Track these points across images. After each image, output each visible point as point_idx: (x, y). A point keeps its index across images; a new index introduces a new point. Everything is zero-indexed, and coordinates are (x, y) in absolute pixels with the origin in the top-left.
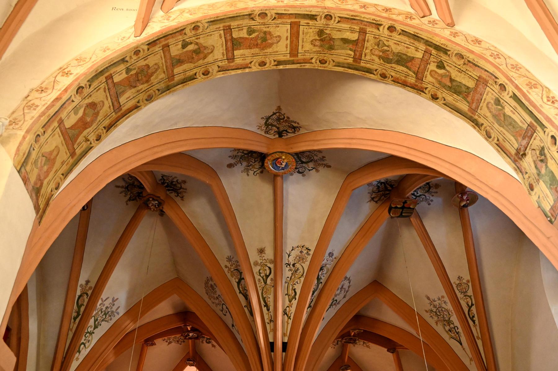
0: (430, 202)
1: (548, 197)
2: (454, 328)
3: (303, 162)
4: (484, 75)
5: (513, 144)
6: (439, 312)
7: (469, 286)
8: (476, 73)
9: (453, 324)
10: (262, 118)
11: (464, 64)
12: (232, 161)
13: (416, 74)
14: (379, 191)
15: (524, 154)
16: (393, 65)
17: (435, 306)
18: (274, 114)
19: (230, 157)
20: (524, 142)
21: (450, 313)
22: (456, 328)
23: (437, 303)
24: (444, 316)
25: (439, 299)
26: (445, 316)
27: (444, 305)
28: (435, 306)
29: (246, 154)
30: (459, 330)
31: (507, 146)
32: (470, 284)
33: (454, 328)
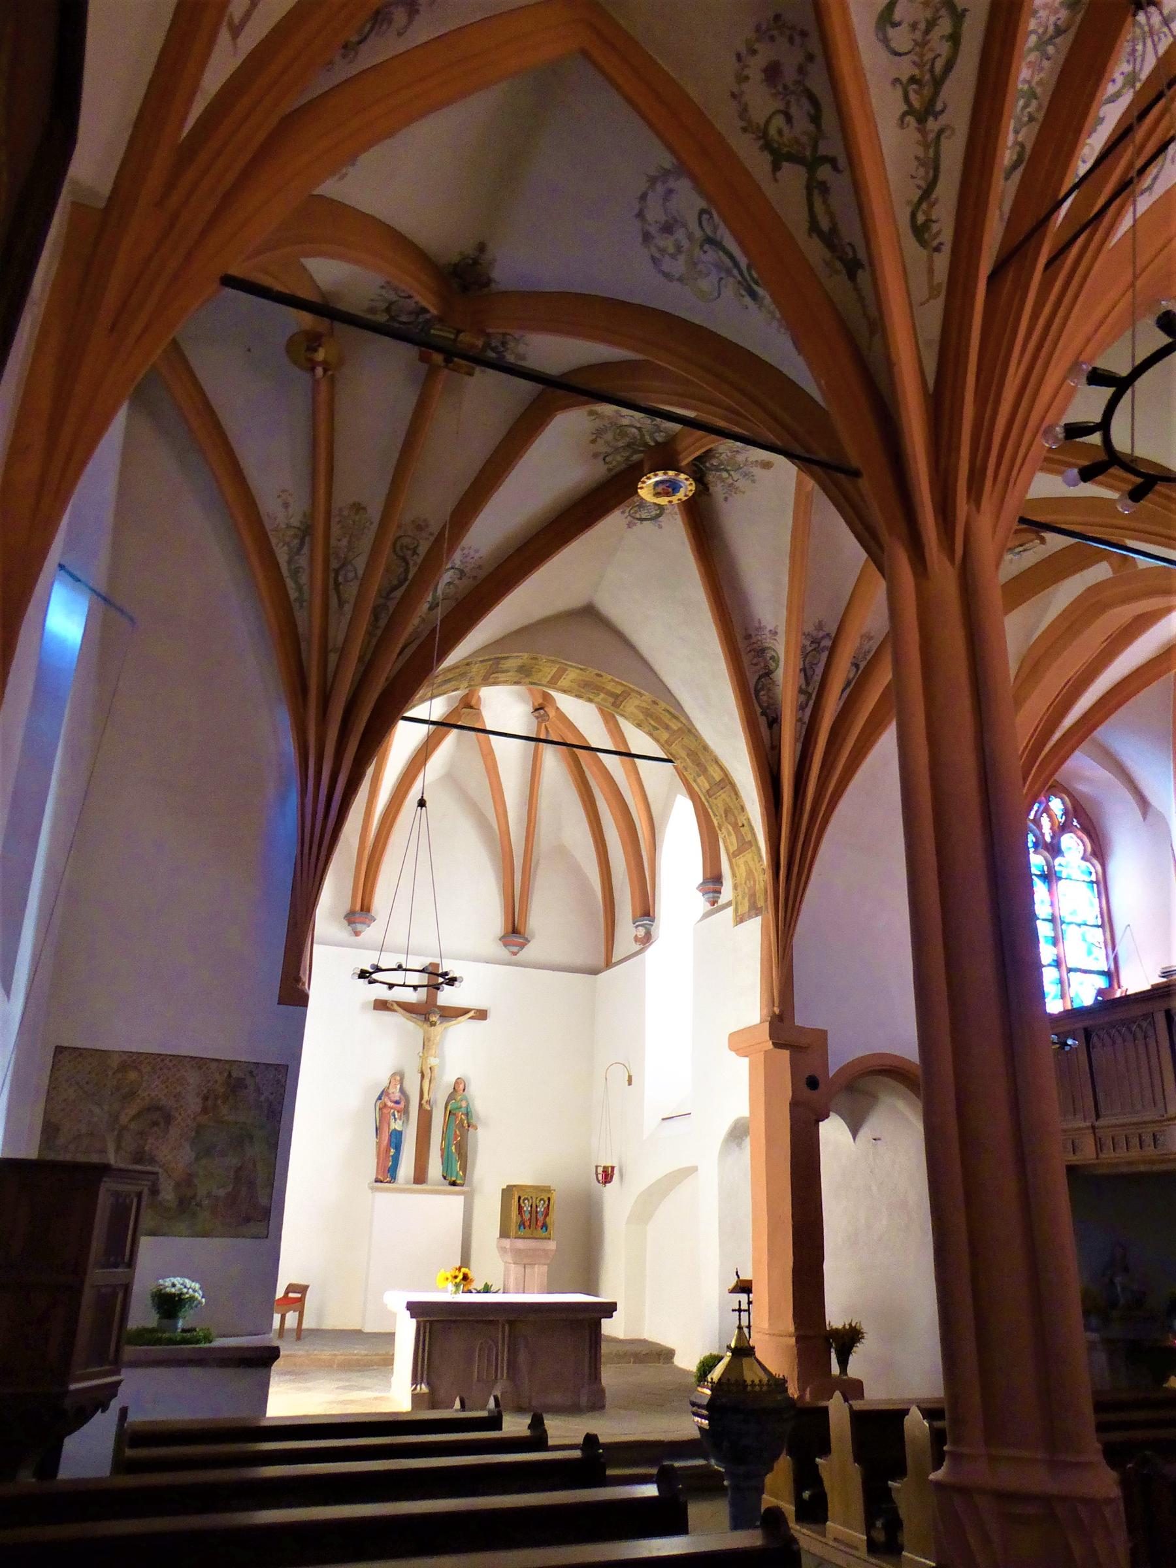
3: (639, 429)
10: (660, 527)
12: (757, 471)
14: (504, 334)
18: (641, 520)
19: (754, 481)
29: (727, 471)
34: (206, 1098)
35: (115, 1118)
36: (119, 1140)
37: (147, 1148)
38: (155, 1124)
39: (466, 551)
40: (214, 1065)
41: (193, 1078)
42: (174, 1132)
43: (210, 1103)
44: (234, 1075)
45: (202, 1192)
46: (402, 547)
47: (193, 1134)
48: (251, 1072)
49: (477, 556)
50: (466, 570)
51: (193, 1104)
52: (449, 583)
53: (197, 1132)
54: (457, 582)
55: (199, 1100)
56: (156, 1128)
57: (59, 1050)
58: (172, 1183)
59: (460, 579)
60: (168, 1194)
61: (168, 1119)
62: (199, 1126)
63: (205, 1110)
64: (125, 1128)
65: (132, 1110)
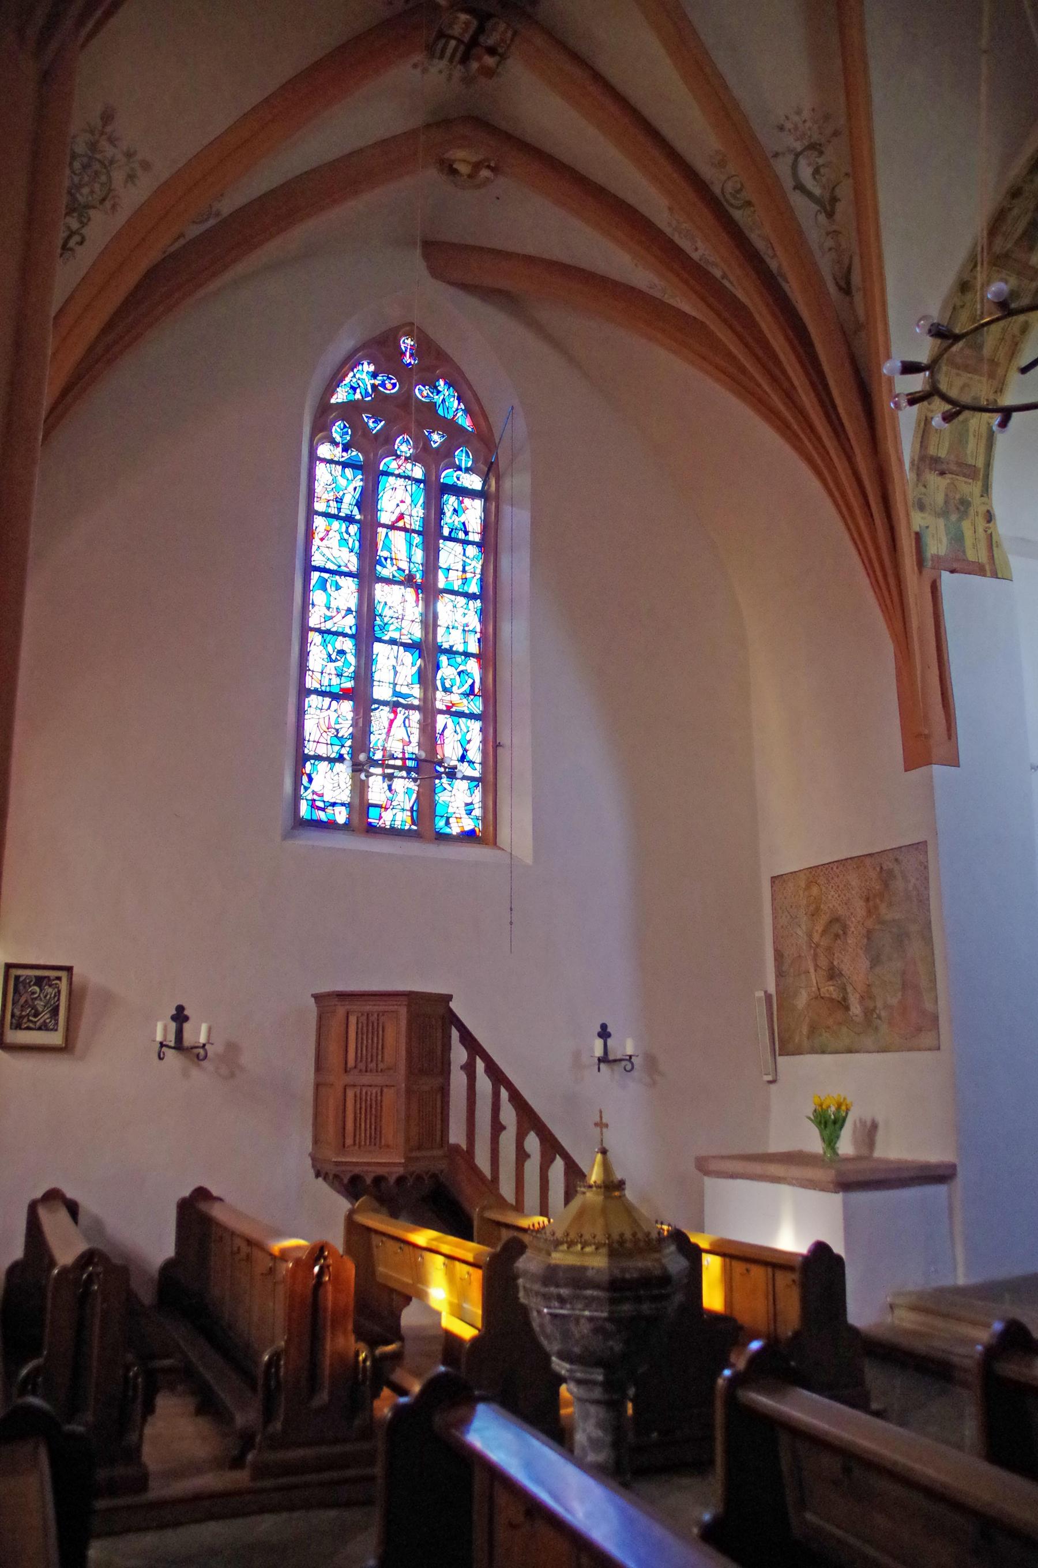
0: (419, 70)
1: (941, 542)
2: (72, 234)
4: (1000, 372)
5: (940, 449)
6: (85, 167)
7: (207, 220)
8: (1001, 355)
9: (83, 225)
11: (1014, 336)
13: (1007, 255)
15: (942, 473)
16: (1030, 214)
17: (93, 146)
20: (954, 468)
21: (108, 204)
22: (76, 238)
23: (109, 151)
24: (79, 187)
25: (129, 155)
26: (85, 190)
27: (118, 176)
28: (93, 146)
30: (79, 250)
31: (933, 439)
32: (212, 222)
33: (72, 234)
34: (868, 900)
35: (810, 936)
36: (815, 957)
37: (835, 963)
38: (837, 936)
39: (789, 125)
40: (868, 861)
41: (853, 879)
42: (851, 941)
43: (871, 903)
44: (885, 867)
45: (879, 1004)
46: (735, 197)
47: (865, 940)
48: (896, 860)
49: (806, 114)
50: (816, 138)
51: (859, 908)
52: (816, 172)
53: (869, 939)
54: (821, 161)
55: (862, 903)
56: (839, 942)
57: (774, 879)
58: (858, 996)
59: (821, 153)
60: (856, 1009)
61: (845, 928)
62: (869, 932)
63: (869, 913)
64: (817, 945)
65: (819, 928)
